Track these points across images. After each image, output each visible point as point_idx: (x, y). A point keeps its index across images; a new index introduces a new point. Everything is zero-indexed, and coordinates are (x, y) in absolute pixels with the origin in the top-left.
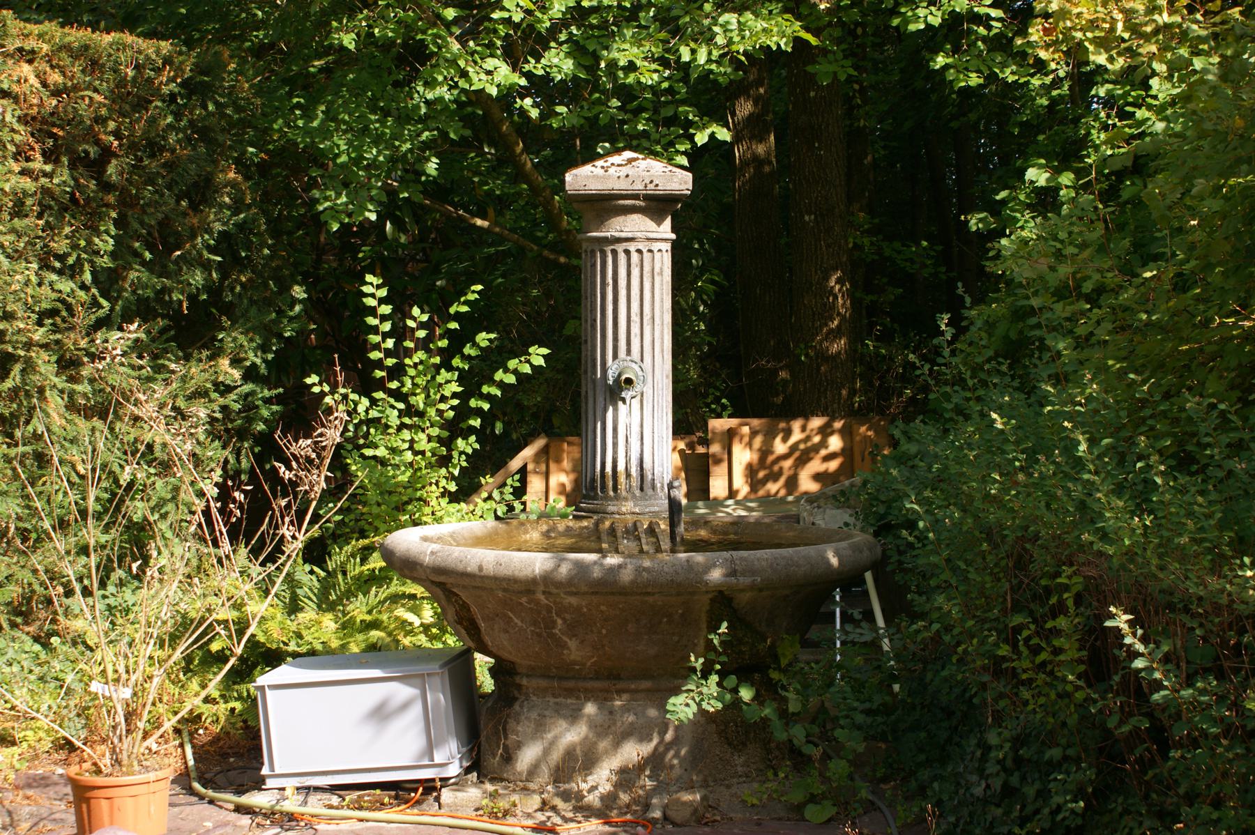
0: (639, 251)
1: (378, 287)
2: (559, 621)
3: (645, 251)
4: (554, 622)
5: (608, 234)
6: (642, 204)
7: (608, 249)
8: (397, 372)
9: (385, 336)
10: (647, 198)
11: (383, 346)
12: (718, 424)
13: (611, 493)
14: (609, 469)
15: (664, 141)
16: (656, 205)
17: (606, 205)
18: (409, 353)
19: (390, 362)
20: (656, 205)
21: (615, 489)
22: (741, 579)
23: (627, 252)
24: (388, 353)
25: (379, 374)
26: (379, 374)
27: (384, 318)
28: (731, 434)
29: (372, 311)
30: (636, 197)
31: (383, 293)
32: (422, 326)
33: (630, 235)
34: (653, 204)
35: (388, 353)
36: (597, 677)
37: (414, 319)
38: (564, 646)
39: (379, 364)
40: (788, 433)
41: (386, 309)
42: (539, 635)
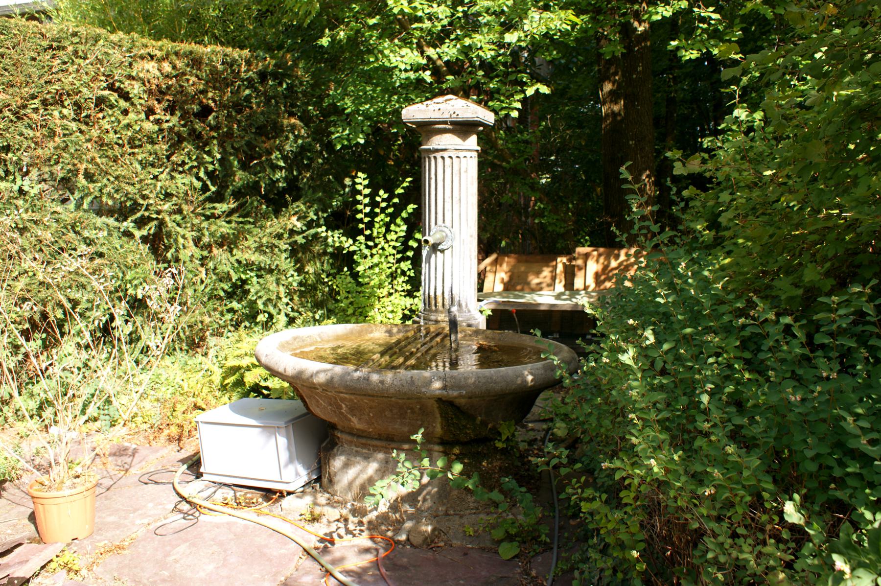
0: (450, 157)
1: (364, 179)
2: (344, 406)
3: (454, 157)
4: (341, 406)
5: (431, 147)
6: (450, 127)
7: (432, 156)
8: (370, 225)
9: (366, 205)
10: (452, 123)
12: (580, 250)
13: (434, 308)
14: (432, 294)
15: (507, 94)
16: (463, 128)
17: (428, 128)
18: (377, 215)
19: (366, 220)
20: (463, 128)
21: (436, 306)
22: (450, 392)
23: (443, 158)
24: (366, 215)
25: (361, 226)
26: (361, 226)
27: (365, 196)
28: (587, 256)
29: (360, 193)
30: (445, 123)
31: (366, 182)
32: (384, 200)
33: (443, 147)
34: (458, 127)
35: (366, 215)
36: (380, 439)
38: (350, 420)
39: (361, 221)
40: (617, 257)
41: (367, 191)
42: (335, 412)
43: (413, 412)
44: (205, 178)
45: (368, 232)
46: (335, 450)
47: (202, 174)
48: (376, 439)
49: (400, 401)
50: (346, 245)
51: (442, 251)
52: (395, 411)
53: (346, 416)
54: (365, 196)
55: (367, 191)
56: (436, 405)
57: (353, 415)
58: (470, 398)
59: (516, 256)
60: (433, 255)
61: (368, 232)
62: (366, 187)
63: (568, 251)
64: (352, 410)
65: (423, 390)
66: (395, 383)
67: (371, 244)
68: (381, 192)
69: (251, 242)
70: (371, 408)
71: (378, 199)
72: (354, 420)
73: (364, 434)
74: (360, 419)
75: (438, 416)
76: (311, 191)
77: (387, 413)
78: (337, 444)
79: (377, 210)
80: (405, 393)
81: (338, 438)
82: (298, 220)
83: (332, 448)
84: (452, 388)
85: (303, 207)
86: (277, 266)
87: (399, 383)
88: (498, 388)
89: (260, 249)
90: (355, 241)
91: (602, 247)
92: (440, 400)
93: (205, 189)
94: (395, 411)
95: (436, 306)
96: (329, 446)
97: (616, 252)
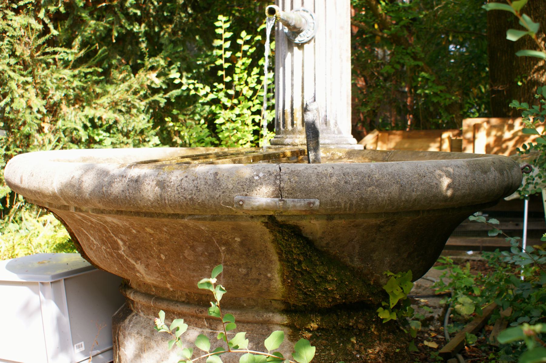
1: (225, 22)
2: (121, 243)
4: (116, 242)
8: (230, 71)
9: (226, 50)
11: (224, 56)
12: (468, 122)
13: (290, 128)
19: (226, 65)
21: (293, 124)
22: (290, 202)
24: (227, 60)
25: (220, 73)
26: (220, 73)
27: (226, 40)
28: (476, 128)
29: (220, 37)
31: (228, 25)
32: (246, 42)
35: (227, 60)
36: (188, 303)
37: (242, 38)
38: (133, 269)
39: (221, 67)
40: (511, 127)
41: (228, 35)
42: (112, 255)
43: (230, 251)
44: (47, 21)
45: (228, 79)
46: (127, 321)
47: (41, 15)
48: (183, 303)
49: (203, 227)
50: (201, 93)
51: (301, 46)
52: (200, 249)
53: (126, 261)
54: (226, 40)
55: (228, 35)
56: (268, 237)
57: (137, 259)
58: (330, 217)
59: (399, 132)
60: (289, 54)
61: (228, 79)
63: (455, 125)
64: (137, 248)
65: (237, 197)
66: (185, 185)
67: (231, 92)
68: (243, 34)
69: (104, 100)
70: (160, 244)
71: (240, 41)
72: (140, 267)
73: (166, 295)
74: (147, 266)
75: (275, 258)
76: (171, 46)
77: (186, 253)
78: (131, 311)
79: (239, 54)
80: (203, 205)
81: (133, 302)
82: (158, 76)
83: (124, 318)
84: (292, 193)
85: (162, 62)
86: (134, 127)
87: (191, 186)
88: (383, 195)
89: (114, 105)
90: (212, 87)
91: (495, 116)
92: (273, 221)
93: (46, 30)
94: (200, 249)
95: (293, 124)
96: (121, 314)
97: (510, 122)
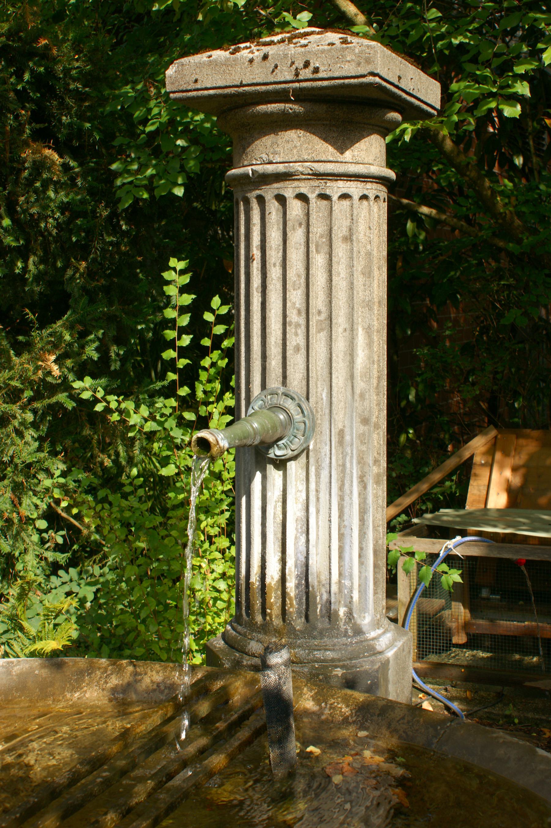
0: (302, 197)
1: (182, 272)
3: (312, 196)
5: (249, 170)
6: (297, 108)
7: (252, 195)
8: (189, 376)
9: (182, 331)
10: (302, 96)
11: (178, 343)
13: (259, 618)
14: (255, 578)
15: (496, 62)
16: (342, 110)
17: (240, 115)
18: (205, 352)
19: (182, 363)
20: (342, 110)
21: (264, 613)
23: (281, 199)
24: (183, 352)
30: (280, 96)
31: (186, 279)
32: (220, 319)
33: (281, 168)
34: (321, 109)
35: (183, 352)
37: (213, 311)
39: (171, 365)
41: (187, 299)
45: (184, 391)
51: (281, 464)
55: (187, 299)
59: (535, 433)
61: (184, 391)
62: (183, 290)
67: (189, 416)
68: (216, 301)
71: (209, 317)
76: (84, 300)
79: (206, 342)
86: (12, 457)
95: (264, 613)
